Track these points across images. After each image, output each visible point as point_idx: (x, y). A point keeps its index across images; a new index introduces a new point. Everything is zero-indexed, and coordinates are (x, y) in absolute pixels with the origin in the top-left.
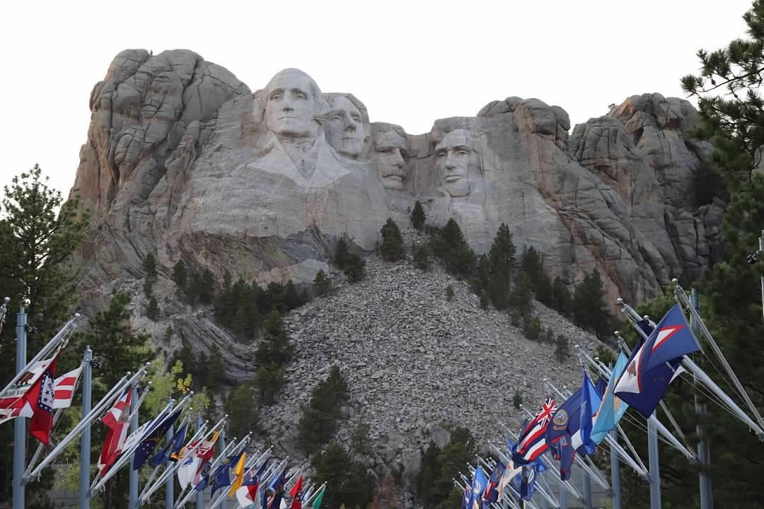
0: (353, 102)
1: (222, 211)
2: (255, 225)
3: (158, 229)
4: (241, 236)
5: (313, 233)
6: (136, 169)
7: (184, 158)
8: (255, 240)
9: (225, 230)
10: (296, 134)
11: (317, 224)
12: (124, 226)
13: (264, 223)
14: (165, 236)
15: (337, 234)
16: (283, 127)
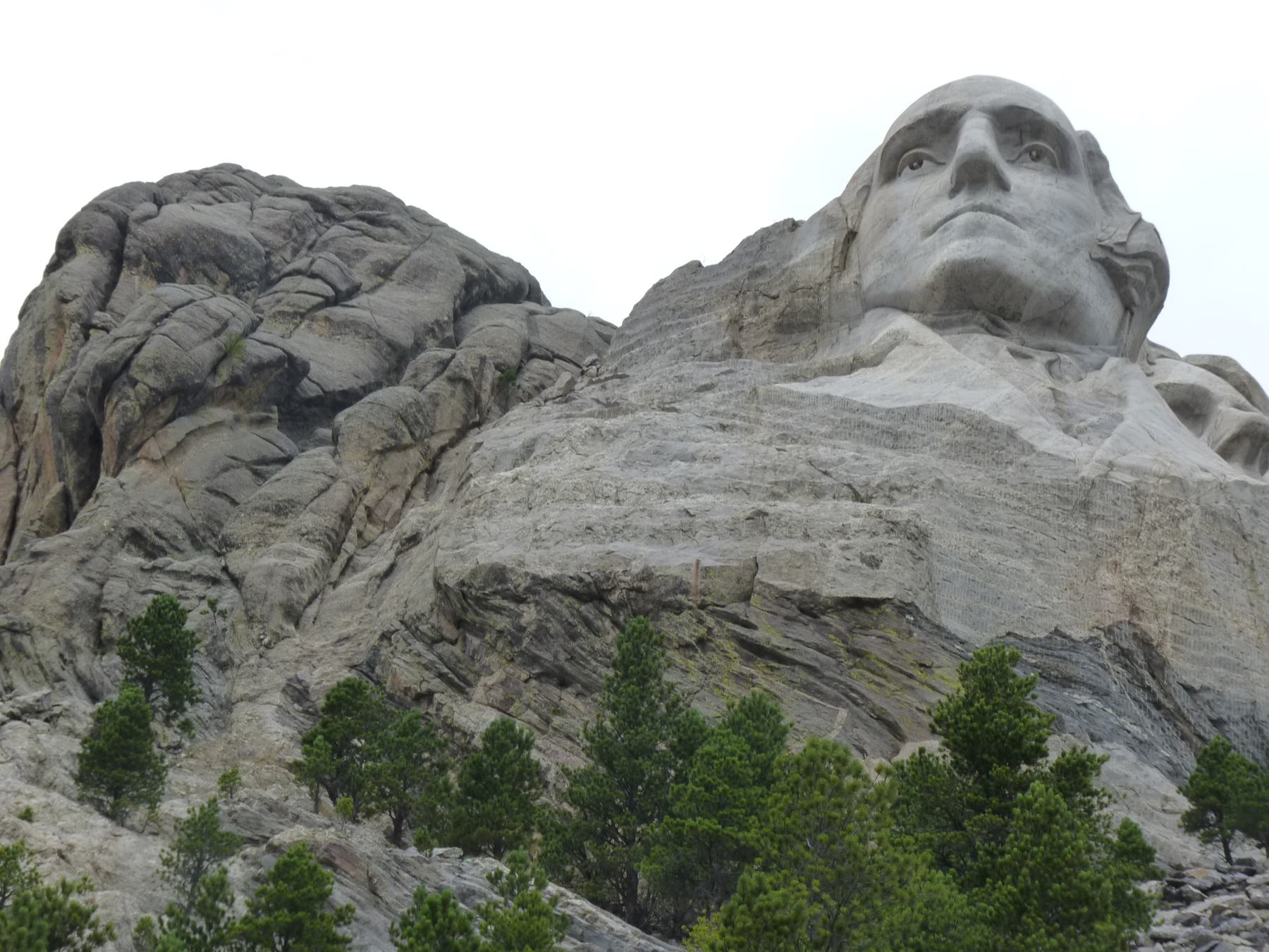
0: (1237, 387)
1: (618, 501)
2: (800, 546)
3: (251, 619)
4: (722, 588)
5: (1125, 666)
6: (184, 424)
7: (435, 400)
8: (809, 608)
9: (627, 562)
10: (1026, 293)
11: (1151, 627)
12: (70, 613)
13: (861, 543)
14: (286, 650)
15: (1261, 700)
16: (953, 249)
